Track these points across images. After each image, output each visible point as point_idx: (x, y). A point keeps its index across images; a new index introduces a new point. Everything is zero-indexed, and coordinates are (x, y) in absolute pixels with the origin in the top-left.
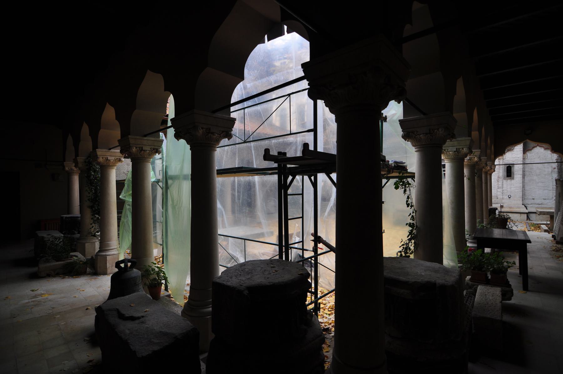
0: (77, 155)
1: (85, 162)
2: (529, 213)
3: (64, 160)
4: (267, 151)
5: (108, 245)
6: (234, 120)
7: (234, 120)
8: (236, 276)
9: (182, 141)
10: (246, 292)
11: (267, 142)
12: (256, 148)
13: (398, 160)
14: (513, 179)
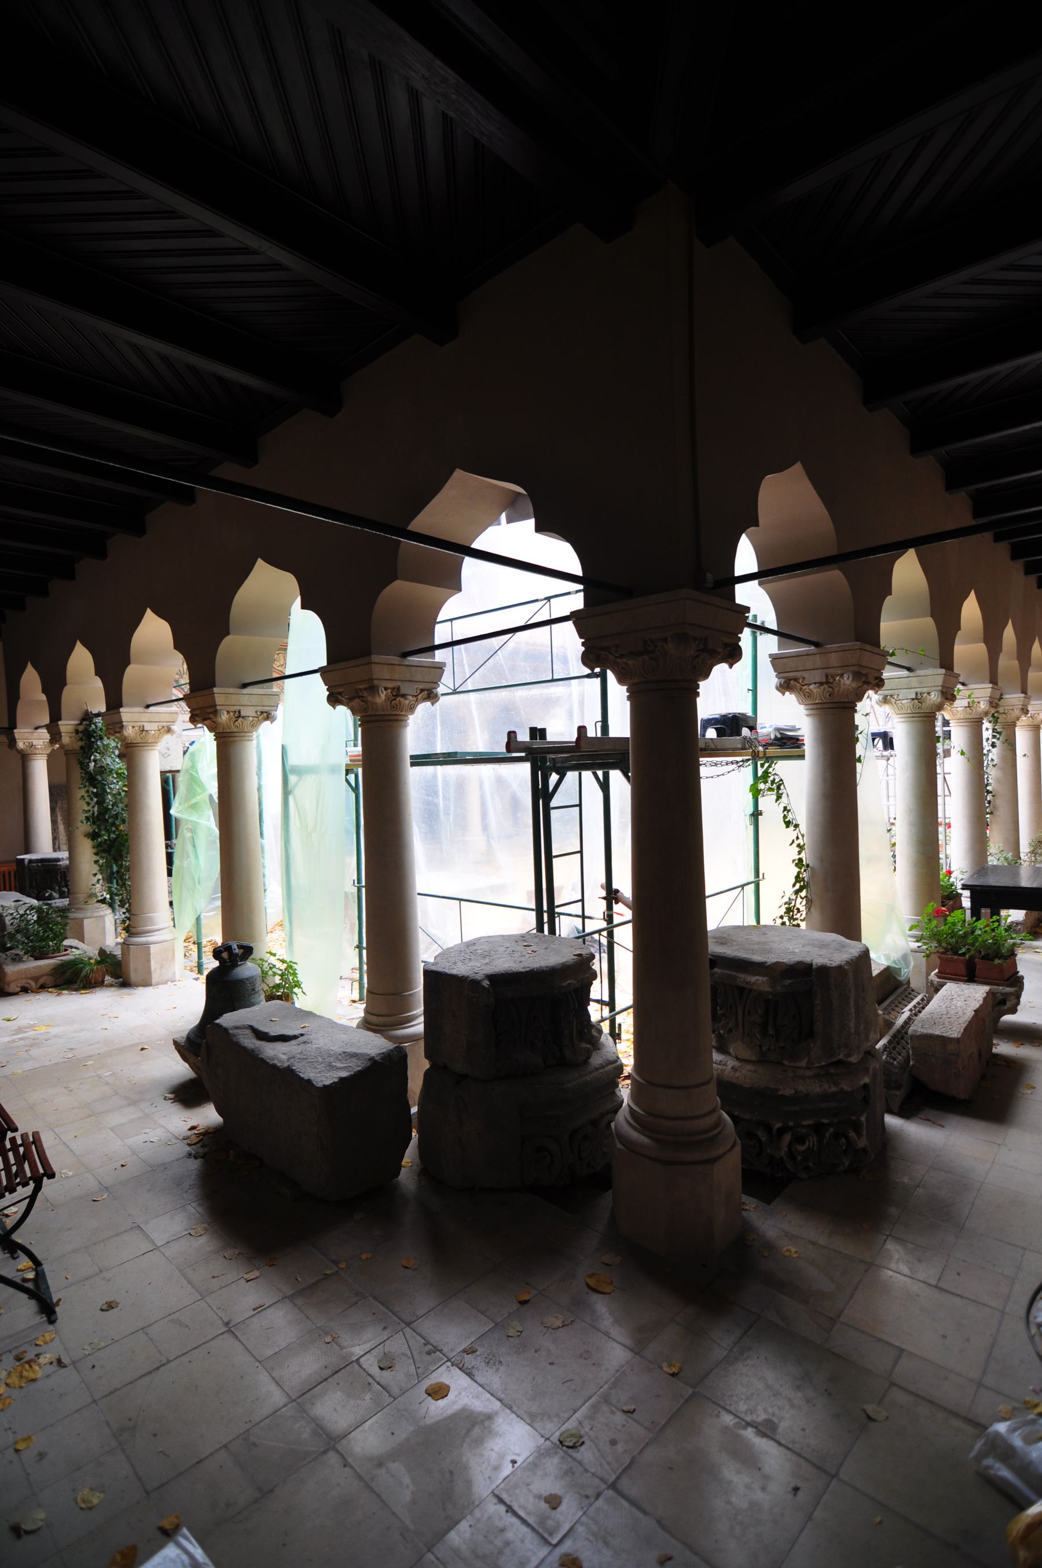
0: (56, 715)
1: (77, 732)
3: (13, 725)
4: (511, 735)
6: (440, 668)
7: (440, 668)
8: (463, 961)
9: (343, 714)
10: (486, 983)
11: (504, 693)
13: (782, 724)
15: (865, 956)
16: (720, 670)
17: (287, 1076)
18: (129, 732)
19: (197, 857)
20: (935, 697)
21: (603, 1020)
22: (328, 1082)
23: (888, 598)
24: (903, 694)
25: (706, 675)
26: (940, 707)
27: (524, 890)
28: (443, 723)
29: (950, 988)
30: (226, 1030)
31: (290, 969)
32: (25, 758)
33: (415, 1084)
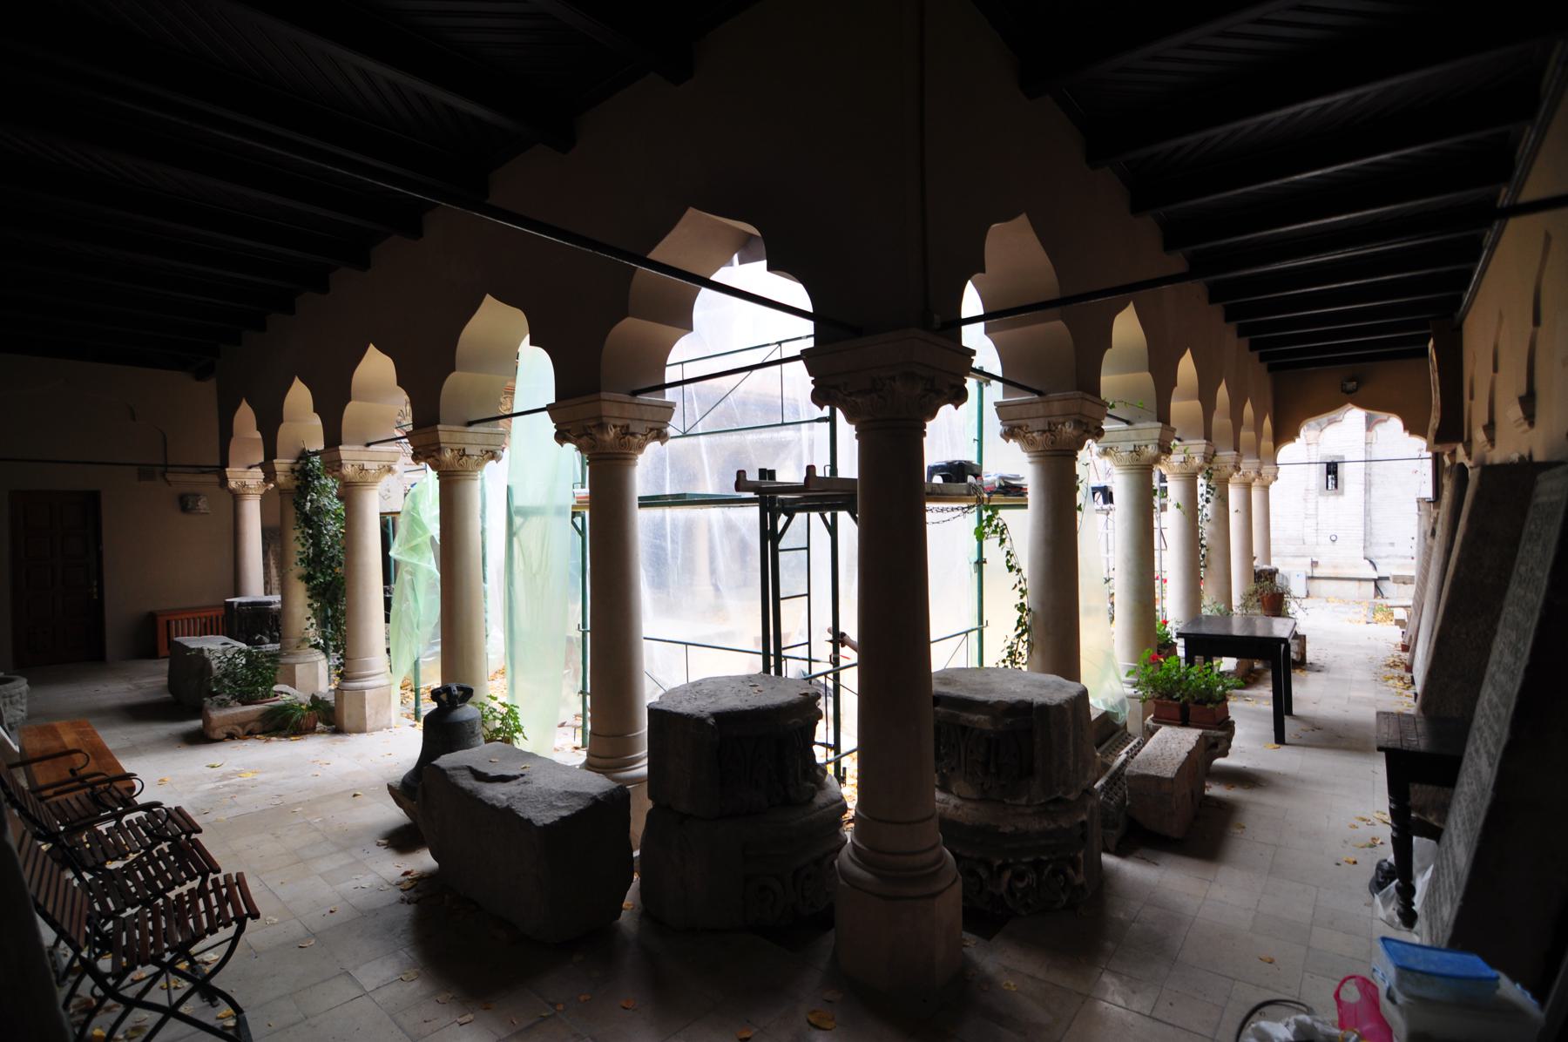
0: (271, 453)
1: (293, 471)
2: (1380, 578)
3: (225, 464)
4: (741, 474)
5: (367, 666)
6: (669, 408)
7: (669, 408)
8: (689, 701)
10: (711, 721)
11: (734, 437)
12: (712, 449)
13: (1007, 473)
14: (1342, 493)
15: (1084, 694)
16: (946, 410)
17: (507, 816)
18: (348, 470)
19: (416, 600)
20: (1152, 450)
21: (828, 762)
22: (548, 821)
23: (1109, 352)
24: (1122, 446)
25: (933, 415)
26: (1157, 460)
27: (750, 631)
28: (673, 465)
29: (1165, 732)
30: (443, 771)
31: (512, 712)
32: (236, 498)
33: (638, 827)
